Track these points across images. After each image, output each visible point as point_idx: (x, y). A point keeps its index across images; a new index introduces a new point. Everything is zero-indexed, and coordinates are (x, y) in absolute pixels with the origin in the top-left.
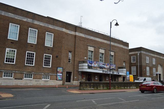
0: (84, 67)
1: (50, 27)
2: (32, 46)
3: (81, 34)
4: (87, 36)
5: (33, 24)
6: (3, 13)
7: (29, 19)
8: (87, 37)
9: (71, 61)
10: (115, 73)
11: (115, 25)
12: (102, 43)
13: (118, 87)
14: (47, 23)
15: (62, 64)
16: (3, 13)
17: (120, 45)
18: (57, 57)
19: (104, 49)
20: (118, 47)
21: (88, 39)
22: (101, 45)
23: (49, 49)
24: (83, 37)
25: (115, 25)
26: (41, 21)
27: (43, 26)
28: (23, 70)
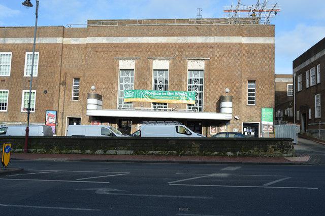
0: (95, 107)
2: (4, 81)
4: (115, 38)
5: (5, 44)
8: (114, 42)
9: (73, 96)
11: (24, 4)
12: (158, 46)
14: (27, 37)
15: (55, 106)
18: (46, 92)
20: (220, 45)
21: (117, 46)
22: (158, 51)
24: (103, 45)
25: (24, 4)
26: (18, 37)
27: (21, 44)
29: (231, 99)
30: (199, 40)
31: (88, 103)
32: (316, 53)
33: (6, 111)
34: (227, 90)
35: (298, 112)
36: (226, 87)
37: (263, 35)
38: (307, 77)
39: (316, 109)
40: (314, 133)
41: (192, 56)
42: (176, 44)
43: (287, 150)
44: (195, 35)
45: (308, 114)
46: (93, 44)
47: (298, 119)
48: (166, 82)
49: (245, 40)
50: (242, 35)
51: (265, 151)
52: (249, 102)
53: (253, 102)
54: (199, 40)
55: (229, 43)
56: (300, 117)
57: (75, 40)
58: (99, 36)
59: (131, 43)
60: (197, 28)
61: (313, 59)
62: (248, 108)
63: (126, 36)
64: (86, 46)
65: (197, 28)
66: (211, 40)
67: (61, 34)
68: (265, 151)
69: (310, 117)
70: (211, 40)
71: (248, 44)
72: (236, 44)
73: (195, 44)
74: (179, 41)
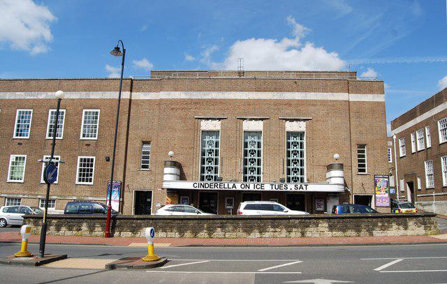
1: (92, 97)
4: (195, 93)
6: (8, 96)
7: (49, 93)
8: (193, 98)
10: (252, 188)
12: (248, 103)
14: (85, 91)
16: (8, 96)
19: (260, 119)
20: (323, 103)
21: (197, 102)
23: (88, 145)
26: (74, 91)
27: (77, 99)
28: (36, 193)
30: (297, 96)
31: (165, 172)
32: (422, 112)
33: (92, 183)
35: (402, 182)
36: (334, 153)
37: (371, 92)
38: (412, 139)
39: (427, 177)
40: (426, 205)
41: (290, 115)
43: (430, 227)
44: (292, 91)
45: (417, 182)
46: (167, 100)
47: (402, 189)
48: (259, 146)
51: (406, 229)
52: (360, 171)
53: (364, 171)
54: (297, 96)
55: (335, 101)
56: (405, 188)
58: (176, 90)
59: (216, 99)
60: (296, 83)
61: (419, 120)
62: (360, 177)
63: (209, 91)
64: (160, 102)
65: (296, 83)
66: (312, 96)
67: (129, 88)
68: (406, 229)
69: (419, 187)
70: (312, 96)
72: (341, 101)
73: (293, 100)
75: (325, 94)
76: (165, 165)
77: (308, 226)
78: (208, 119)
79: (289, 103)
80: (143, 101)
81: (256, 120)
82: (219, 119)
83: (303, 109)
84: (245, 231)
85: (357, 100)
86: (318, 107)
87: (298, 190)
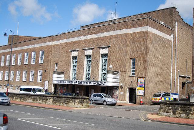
3: (65, 40)
4: (70, 39)
5: (34, 48)
12: (87, 41)
13: (16, 99)
17: (120, 31)
20: (116, 36)
23: (41, 66)
29: (113, 72)
30: (105, 34)
34: (111, 66)
41: (101, 45)
42: (95, 38)
46: (62, 44)
49: (129, 31)
50: (127, 28)
54: (105, 34)
55: (121, 34)
57: (57, 42)
58: (65, 39)
60: (105, 27)
66: (112, 33)
70: (112, 33)
71: (132, 34)
72: (124, 34)
74: (97, 37)
75: (117, 31)
76: (54, 73)
77: (47, 100)
78: (74, 51)
79: (101, 39)
80: (56, 45)
81: (89, 49)
82: (78, 51)
83: (107, 41)
84: (33, 100)
85: (133, 32)
86: (113, 39)
87: (101, 85)
